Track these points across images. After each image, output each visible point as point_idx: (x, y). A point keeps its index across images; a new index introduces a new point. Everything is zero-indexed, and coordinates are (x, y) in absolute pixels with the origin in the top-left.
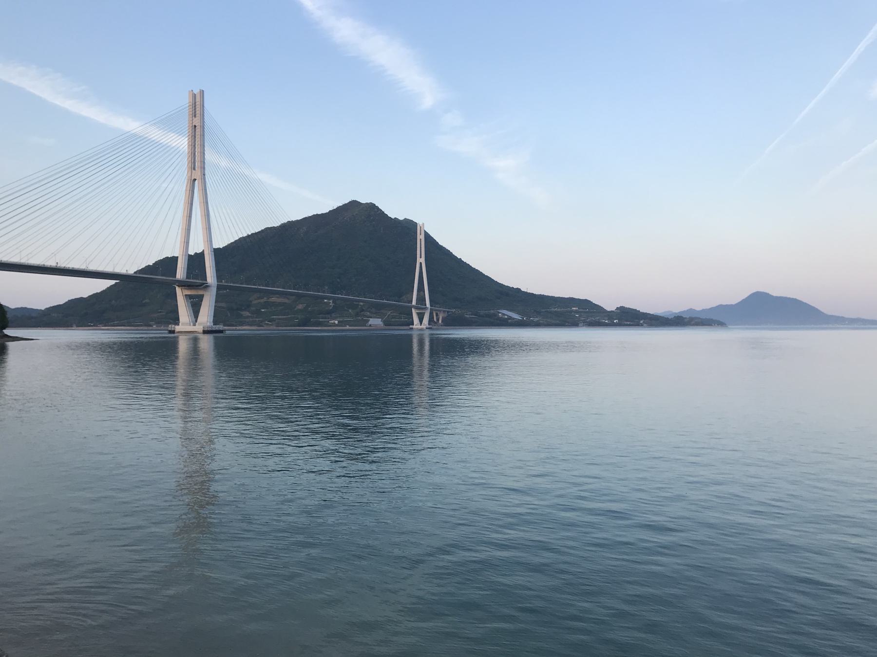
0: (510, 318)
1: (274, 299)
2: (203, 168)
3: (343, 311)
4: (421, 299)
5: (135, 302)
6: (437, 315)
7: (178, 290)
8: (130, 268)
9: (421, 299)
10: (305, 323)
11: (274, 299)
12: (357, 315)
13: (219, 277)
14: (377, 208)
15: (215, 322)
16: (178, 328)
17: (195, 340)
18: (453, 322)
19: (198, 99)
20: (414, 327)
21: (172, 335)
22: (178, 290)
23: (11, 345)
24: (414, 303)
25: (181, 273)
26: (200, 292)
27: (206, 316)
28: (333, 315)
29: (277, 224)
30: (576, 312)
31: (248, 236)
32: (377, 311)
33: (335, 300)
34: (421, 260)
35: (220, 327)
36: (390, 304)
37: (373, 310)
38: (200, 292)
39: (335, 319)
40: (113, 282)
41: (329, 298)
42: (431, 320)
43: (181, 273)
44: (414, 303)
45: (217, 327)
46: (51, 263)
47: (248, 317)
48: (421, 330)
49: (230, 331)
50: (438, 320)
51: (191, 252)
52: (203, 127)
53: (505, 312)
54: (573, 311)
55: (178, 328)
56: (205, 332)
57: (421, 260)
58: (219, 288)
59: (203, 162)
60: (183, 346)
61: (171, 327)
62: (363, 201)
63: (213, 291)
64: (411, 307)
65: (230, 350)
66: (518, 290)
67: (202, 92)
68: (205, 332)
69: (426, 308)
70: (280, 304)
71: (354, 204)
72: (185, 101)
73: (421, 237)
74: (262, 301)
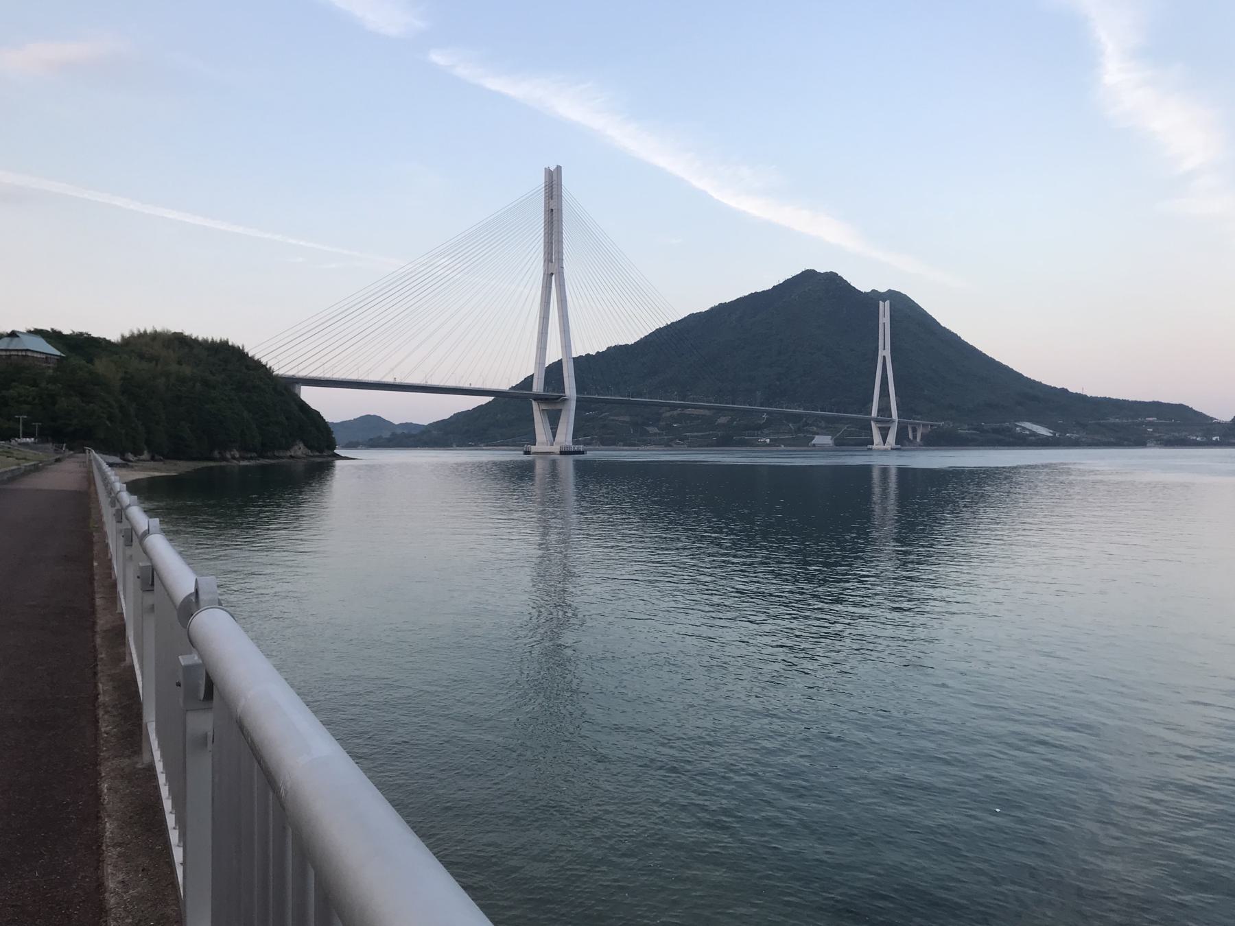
0: (1034, 434)
1: (689, 411)
2: (560, 260)
3: (796, 428)
4: (884, 409)
5: (499, 420)
6: (914, 430)
7: (535, 404)
8: (506, 381)
9: (884, 409)
10: (725, 442)
11: (689, 411)
12: (799, 430)
13: (580, 389)
14: (841, 278)
15: (575, 442)
16: (534, 449)
17: (554, 463)
18: (937, 440)
19: (555, 178)
20: (874, 447)
21: (527, 458)
22: (535, 404)
23: (338, 463)
24: (874, 413)
25: (538, 387)
26: (558, 407)
27: (565, 435)
28: (766, 431)
29: (703, 307)
30: (1151, 424)
31: (667, 327)
32: (829, 426)
33: (769, 413)
34: (885, 352)
35: (581, 448)
36: (843, 418)
37: (823, 424)
38: (558, 407)
39: (766, 436)
40: (491, 398)
41: (764, 411)
42: (902, 439)
43: (538, 387)
44: (874, 413)
45: (576, 448)
46: (389, 379)
47: (655, 434)
48: (886, 450)
49: (596, 454)
50: (915, 437)
51: (551, 359)
52: (560, 210)
53: (1028, 425)
54: (1143, 423)
55: (534, 449)
56: (562, 453)
57: (885, 352)
58: (578, 400)
59: (560, 253)
60: (540, 467)
61: (526, 448)
62: (821, 269)
63: (573, 405)
64: (869, 421)
65: (588, 473)
66: (1064, 391)
67: (559, 168)
68: (562, 453)
69: (892, 421)
70: (698, 417)
71: (809, 275)
72: (540, 181)
73: (885, 320)
74: (675, 413)
